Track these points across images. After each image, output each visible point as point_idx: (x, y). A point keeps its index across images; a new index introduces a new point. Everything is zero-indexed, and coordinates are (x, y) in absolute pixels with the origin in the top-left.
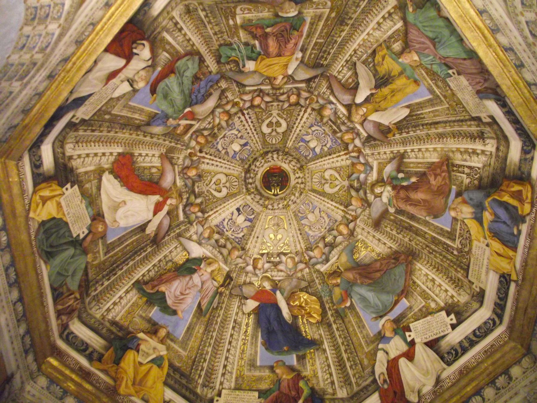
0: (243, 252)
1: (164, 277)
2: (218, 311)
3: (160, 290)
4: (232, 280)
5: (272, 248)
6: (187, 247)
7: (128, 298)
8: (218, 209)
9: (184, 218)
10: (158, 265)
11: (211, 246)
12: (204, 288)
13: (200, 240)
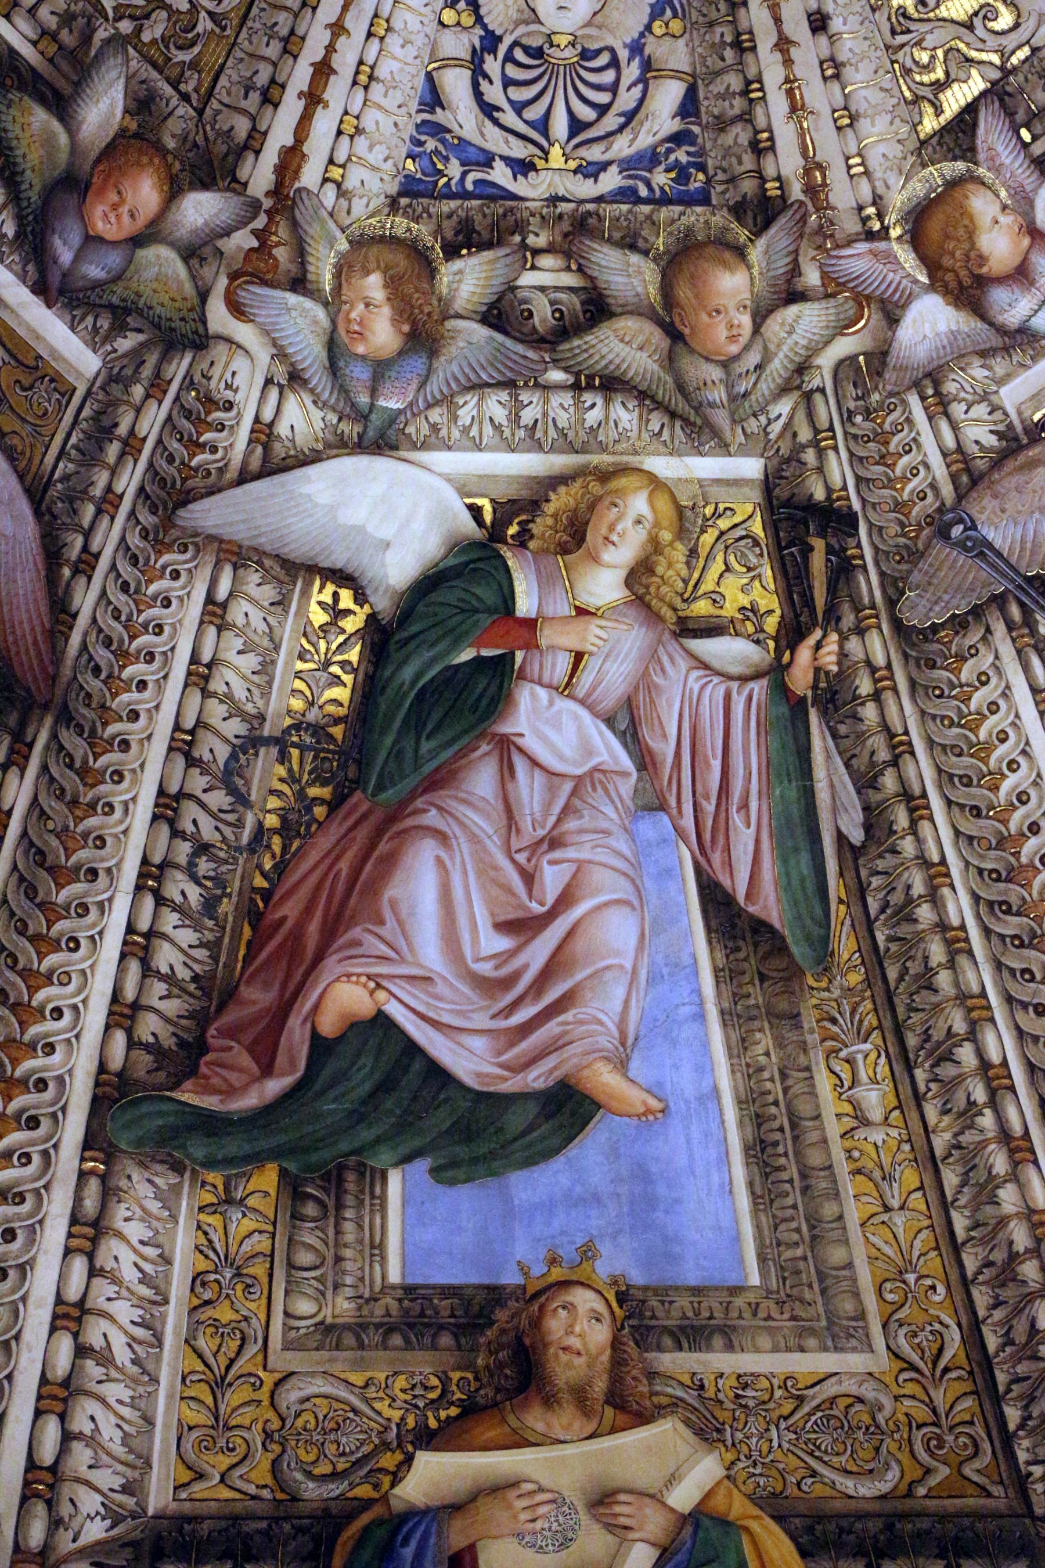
0: (778, 235)
1: (290, 910)
2: (908, 846)
3: (328, 1025)
4: (850, 521)
5: (1005, 19)
6: (298, 549)
7: (130, 1275)
8: (313, 50)
9: (95, 340)
10: (183, 850)
11: (478, 386)
12: (665, 750)
13: (362, 417)
